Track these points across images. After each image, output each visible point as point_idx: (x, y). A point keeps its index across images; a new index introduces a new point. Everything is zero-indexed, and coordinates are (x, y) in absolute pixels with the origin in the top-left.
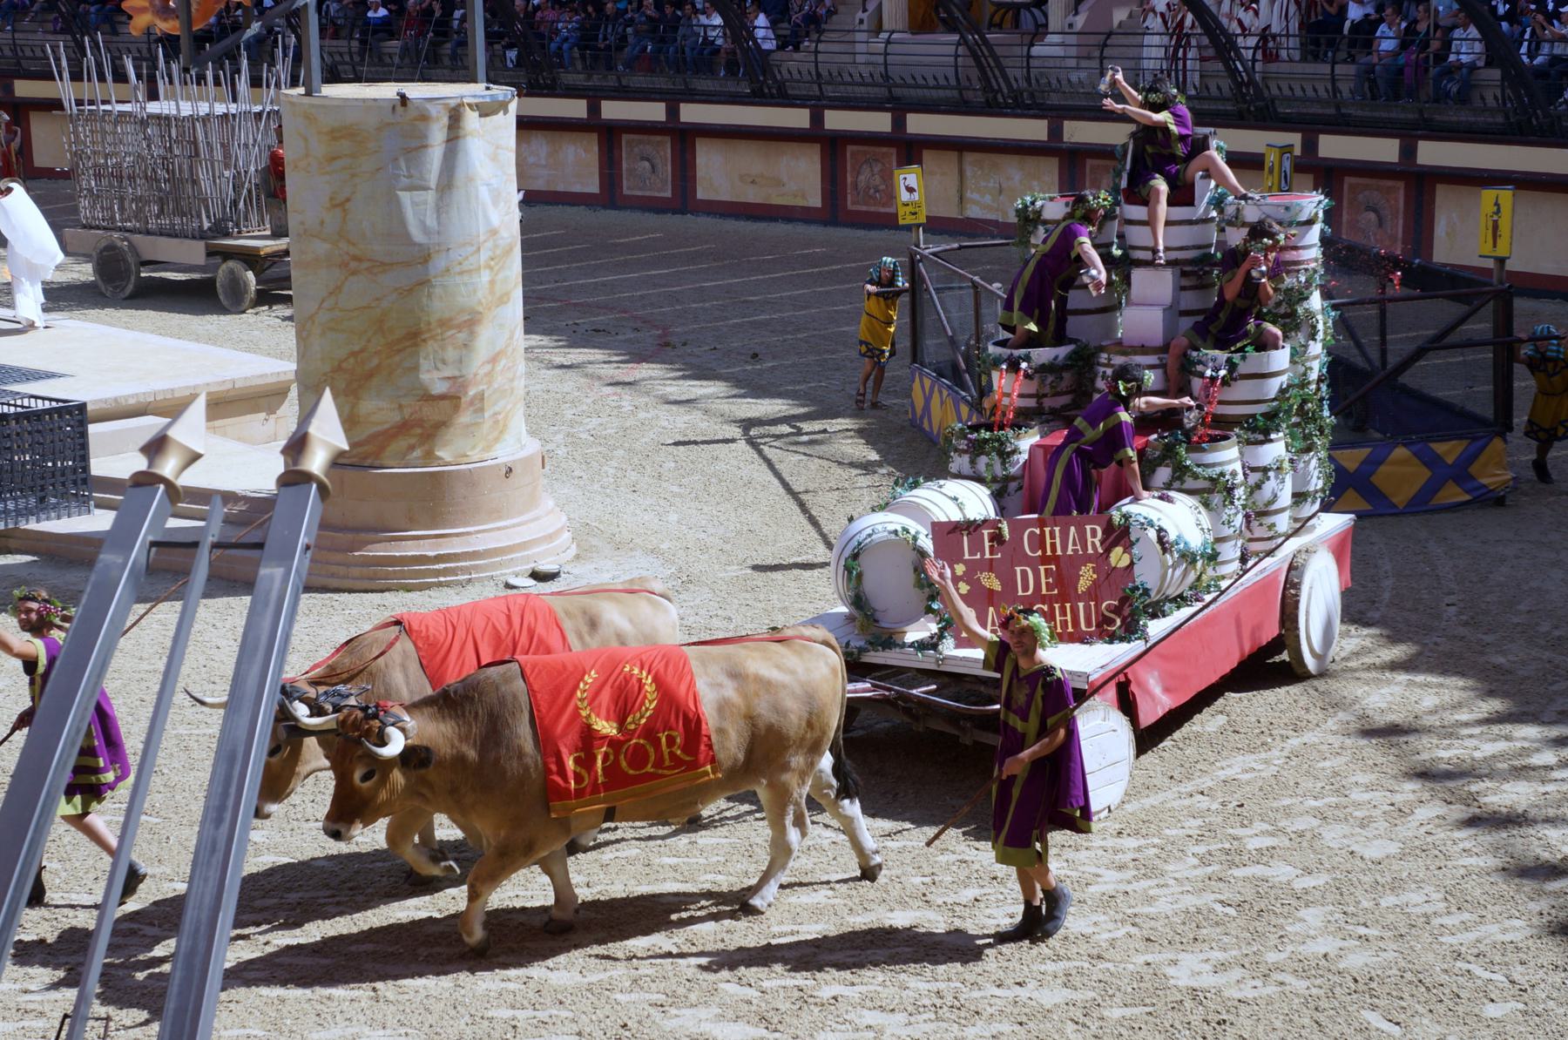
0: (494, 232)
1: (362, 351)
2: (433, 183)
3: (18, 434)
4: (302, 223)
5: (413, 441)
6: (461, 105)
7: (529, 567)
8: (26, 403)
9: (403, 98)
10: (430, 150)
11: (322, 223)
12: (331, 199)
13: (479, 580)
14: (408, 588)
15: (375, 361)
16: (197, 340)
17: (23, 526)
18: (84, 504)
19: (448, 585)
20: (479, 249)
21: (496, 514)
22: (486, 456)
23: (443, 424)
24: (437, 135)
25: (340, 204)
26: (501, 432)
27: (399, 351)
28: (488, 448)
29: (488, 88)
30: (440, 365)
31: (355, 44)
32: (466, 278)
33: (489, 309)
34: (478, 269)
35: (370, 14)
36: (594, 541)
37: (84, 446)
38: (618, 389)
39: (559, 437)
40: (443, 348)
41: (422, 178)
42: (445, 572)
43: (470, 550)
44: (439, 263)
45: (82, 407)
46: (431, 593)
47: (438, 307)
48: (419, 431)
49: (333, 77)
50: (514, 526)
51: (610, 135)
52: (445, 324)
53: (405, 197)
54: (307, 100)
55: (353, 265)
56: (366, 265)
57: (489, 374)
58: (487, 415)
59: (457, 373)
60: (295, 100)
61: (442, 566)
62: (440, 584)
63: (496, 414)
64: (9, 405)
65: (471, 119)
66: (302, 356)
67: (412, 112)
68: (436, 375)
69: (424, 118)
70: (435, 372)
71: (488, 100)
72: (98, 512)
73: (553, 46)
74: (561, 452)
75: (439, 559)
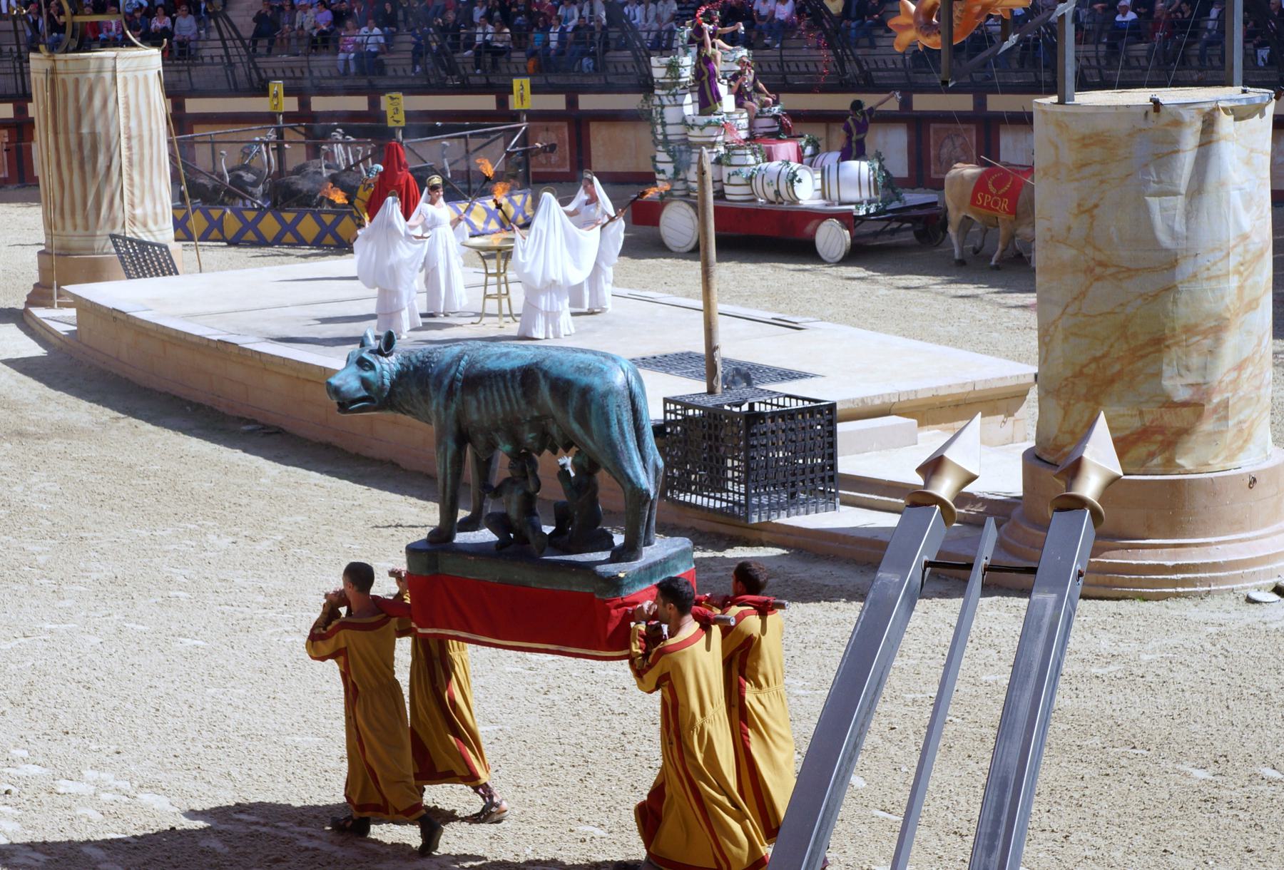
0: (1245, 237)
1: (1104, 356)
2: (1183, 190)
3: (773, 432)
4: (1049, 229)
5: (1153, 448)
7: (1273, 581)
8: (781, 403)
9: (1156, 104)
10: (1181, 155)
11: (1069, 229)
12: (1079, 205)
13: (1220, 592)
14: (1145, 598)
15: (1117, 367)
16: (939, 341)
17: (775, 520)
18: (830, 500)
19: (1186, 596)
20: (1228, 254)
22: (1228, 465)
24: (1190, 140)
25: (1088, 211)
26: (1246, 441)
27: (1142, 357)
28: (1231, 457)
29: (1244, 92)
30: (1183, 372)
31: (1102, 48)
32: (1213, 283)
33: (1237, 315)
34: (1227, 274)
35: (1119, 18)
37: (833, 445)
41: (1172, 183)
42: (1184, 583)
43: (1210, 561)
44: (1186, 268)
45: (832, 407)
46: (1169, 603)
47: (1183, 312)
48: (1159, 438)
50: (1257, 538)
52: (1190, 330)
53: (1154, 202)
54: (1060, 108)
55: (1098, 270)
56: (1112, 270)
57: (1234, 381)
58: (1231, 423)
59: (1201, 380)
60: (1047, 109)
61: (1180, 576)
62: (1178, 595)
63: (1240, 422)
64: (766, 403)
65: (1226, 124)
66: (1043, 361)
67: (1164, 118)
68: (1179, 381)
69: (1178, 123)
70: (1178, 379)
71: (1244, 103)
72: (843, 508)
75: (1177, 569)
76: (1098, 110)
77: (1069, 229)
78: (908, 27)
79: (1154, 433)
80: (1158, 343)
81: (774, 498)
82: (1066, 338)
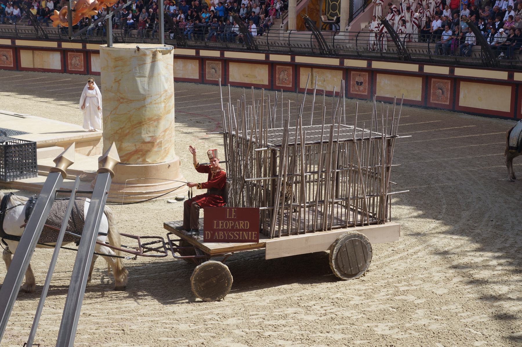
0: (166, 91)
1: (124, 127)
2: (147, 75)
4: (106, 87)
5: (139, 156)
6: (157, 51)
7: (175, 196)
8: (17, 142)
9: (138, 48)
11: (112, 87)
12: (115, 80)
13: (159, 200)
15: (128, 131)
16: (72, 123)
17: (15, 180)
18: (35, 174)
22: (162, 161)
23: (148, 151)
24: (149, 60)
25: (118, 81)
26: (167, 154)
27: (135, 128)
28: (163, 159)
29: (165, 46)
31: (123, 31)
32: (157, 105)
34: (161, 102)
35: (128, 22)
37: (35, 156)
38: (204, 141)
39: (185, 156)
40: (149, 127)
44: (148, 100)
45: (35, 143)
47: (148, 114)
48: (141, 153)
49: (116, 41)
51: (202, 61)
52: (150, 119)
53: (138, 79)
54: (108, 48)
55: (121, 100)
56: (125, 100)
57: (163, 135)
58: (163, 148)
59: (153, 135)
60: (104, 48)
63: (165, 148)
64: (12, 142)
65: (160, 56)
68: (147, 135)
69: (145, 55)
72: (39, 176)
73: (185, 33)
74: (186, 160)
76: (120, 50)
78: (57, 19)
79: (139, 151)
80: (140, 123)
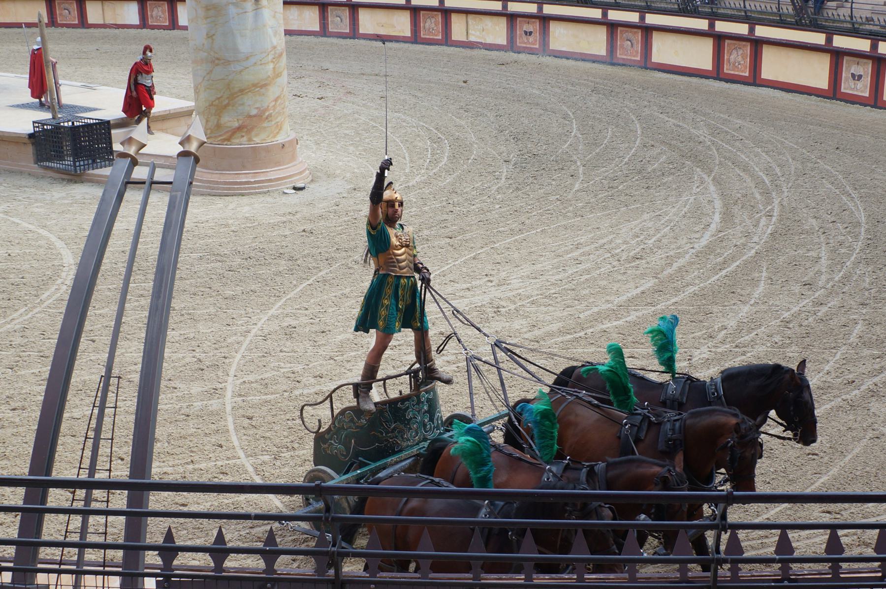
1: (221, 97)
4: (195, 45)
11: (203, 45)
12: (207, 34)
21: (278, 164)
22: (273, 140)
26: (279, 130)
28: (275, 137)
33: (273, 79)
36: (319, 174)
45: (108, 122)
55: (217, 62)
56: (223, 61)
57: (274, 106)
75: (255, 182)
77: (203, 45)
79: (243, 128)
81: (86, 162)
82: (205, 90)
